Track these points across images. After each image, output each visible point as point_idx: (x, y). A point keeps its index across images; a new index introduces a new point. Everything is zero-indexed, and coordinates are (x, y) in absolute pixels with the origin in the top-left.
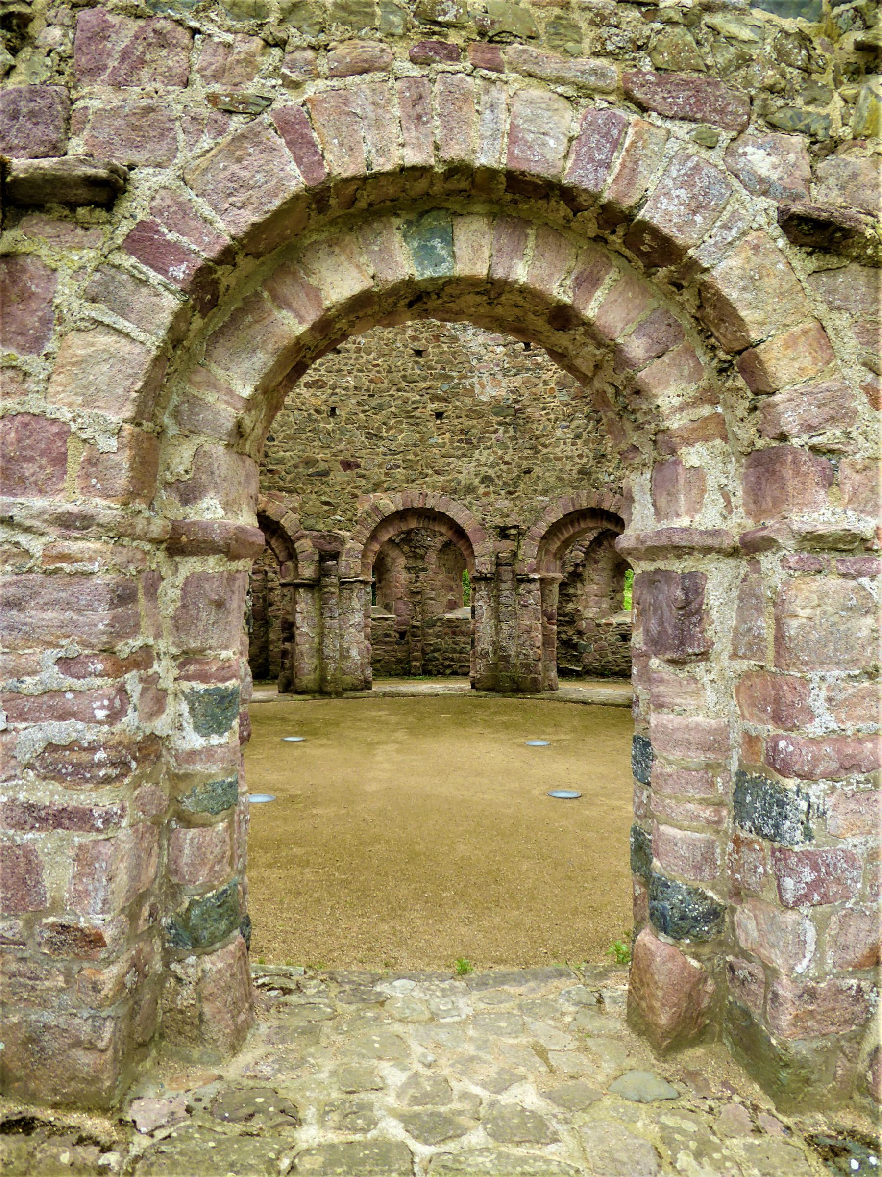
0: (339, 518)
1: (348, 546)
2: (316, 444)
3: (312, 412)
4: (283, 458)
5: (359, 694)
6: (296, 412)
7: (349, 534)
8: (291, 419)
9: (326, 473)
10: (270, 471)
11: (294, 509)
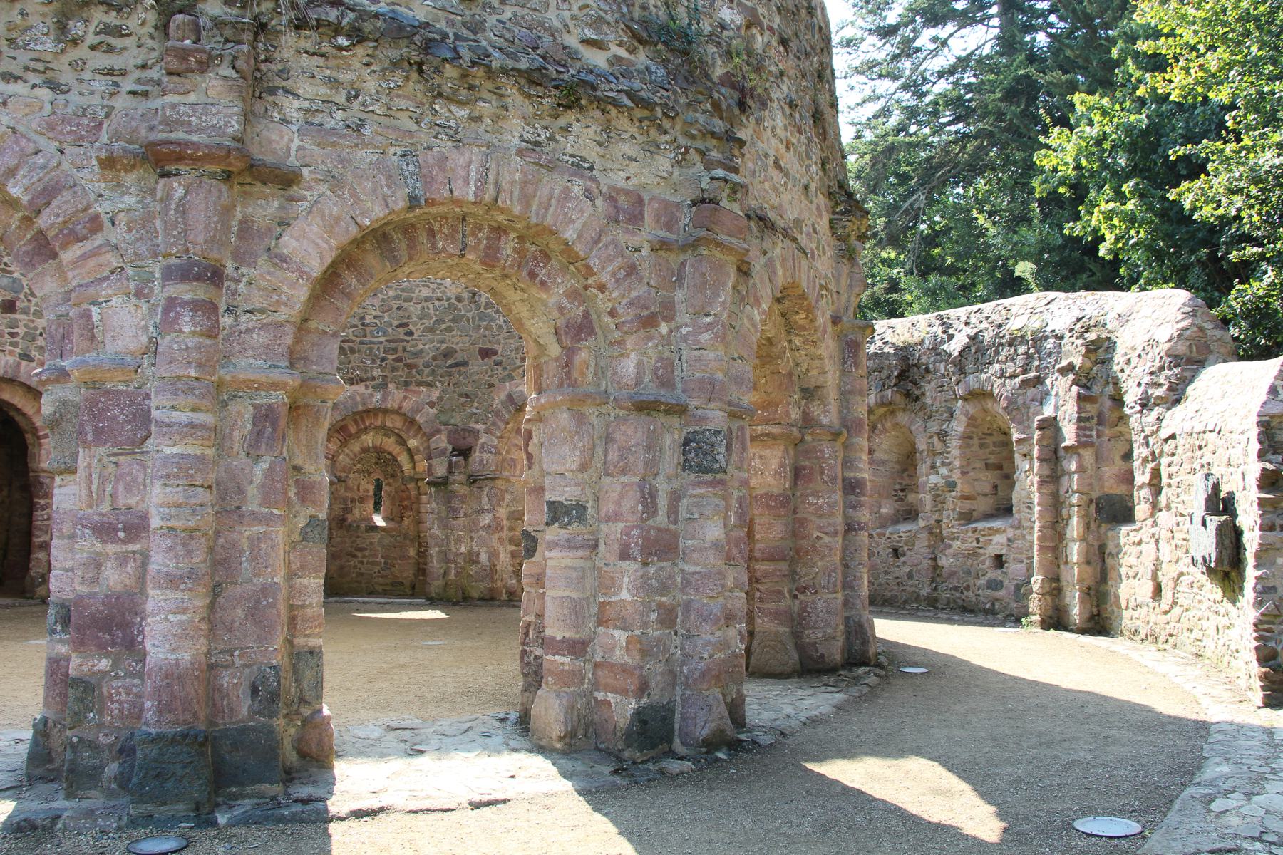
0: (475, 410)
1: (482, 440)
2: (454, 333)
3: (453, 301)
4: (421, 351)
5: (479, 603)
6: (437, 303)
7: (484, 427)
8: (431, 311)
9: (465, 364)
10: (409, 366)
11: (432, 405)
